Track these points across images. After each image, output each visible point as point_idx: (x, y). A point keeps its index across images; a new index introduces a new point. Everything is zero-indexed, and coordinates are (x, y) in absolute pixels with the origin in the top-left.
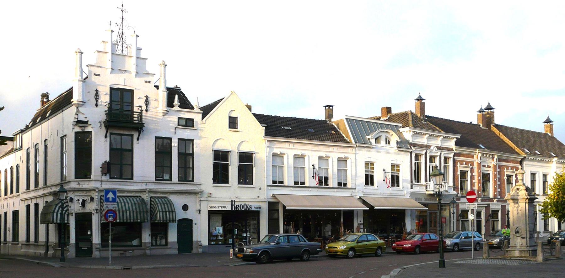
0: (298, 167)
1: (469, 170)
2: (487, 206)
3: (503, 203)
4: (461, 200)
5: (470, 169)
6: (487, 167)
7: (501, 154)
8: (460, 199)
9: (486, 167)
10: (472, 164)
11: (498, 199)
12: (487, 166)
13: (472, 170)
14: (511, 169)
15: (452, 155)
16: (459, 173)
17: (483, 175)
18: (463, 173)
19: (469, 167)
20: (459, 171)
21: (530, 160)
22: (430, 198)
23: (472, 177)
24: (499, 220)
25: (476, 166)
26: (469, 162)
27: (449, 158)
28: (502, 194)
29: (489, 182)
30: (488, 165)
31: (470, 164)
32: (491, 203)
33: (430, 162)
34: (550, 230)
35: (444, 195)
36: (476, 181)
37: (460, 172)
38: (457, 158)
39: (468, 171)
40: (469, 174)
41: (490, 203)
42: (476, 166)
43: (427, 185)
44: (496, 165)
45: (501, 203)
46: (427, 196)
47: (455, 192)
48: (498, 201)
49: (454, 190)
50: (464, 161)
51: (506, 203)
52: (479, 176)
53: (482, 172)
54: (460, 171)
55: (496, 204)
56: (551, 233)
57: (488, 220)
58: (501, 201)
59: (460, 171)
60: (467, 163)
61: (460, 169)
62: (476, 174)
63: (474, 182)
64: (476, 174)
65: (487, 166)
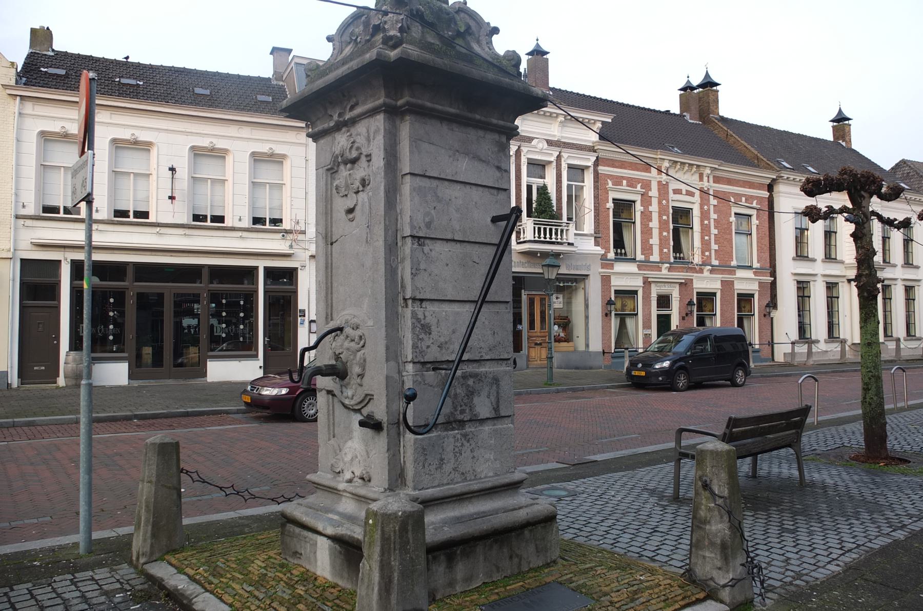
0: (128, 174)
1: (638, 198)
2: (683, 281)
3: (727, 277)
4: (615, 268)
5: (640, 196)
6: (686, 195)
7: (719, 166)
8: (612, 265)
9: (681, 194)
10: (647, 185)
11: (712, 266)
12: (684, 192)
13: (646, 200)
14: (746, 201)
15: (590, 163)
16: (610, 205)
17: (673, 212)
18: (623, 207)
19: (636, 193)
20: (611, 200)
21: (793, 182)
22: (529, 262)
23: (647, 216)
24: (715, 314)
25: (654, 192)
26: (639, 181)
27: (582, 169)
28: (725, 253)
29: (692, 228)
30: (686, 190)
31: (639, 186)
32: (695, 275)
33: (528, 176)
34: (841, 337)
35: (563, 254)
36: (654, 224)
37: (613, 203)
38: (602, 169)
39: (634, 202)
40: (639, 207)
41: (693, 276)
42: (654, 192)
43: (520, 229)
44: (708, 189)
45: (721, 276)
46: (519, 254)
47: (599, 248)
48: (711, 272)
49: (597, 244)
50: (623, 178)
51: (734, 276)
52: (662, 211)
53: (672, 204)
54: (613, 199)
55: (705, 278)
56: (843, 342)
57: (687, 314)
58: (723, 272)
59: (614, 199)
60: (632, 182)
61: (612, 195)
62: (654, 207)
63: (650, 226)
64: (654, 207)
65: (684, 192)
